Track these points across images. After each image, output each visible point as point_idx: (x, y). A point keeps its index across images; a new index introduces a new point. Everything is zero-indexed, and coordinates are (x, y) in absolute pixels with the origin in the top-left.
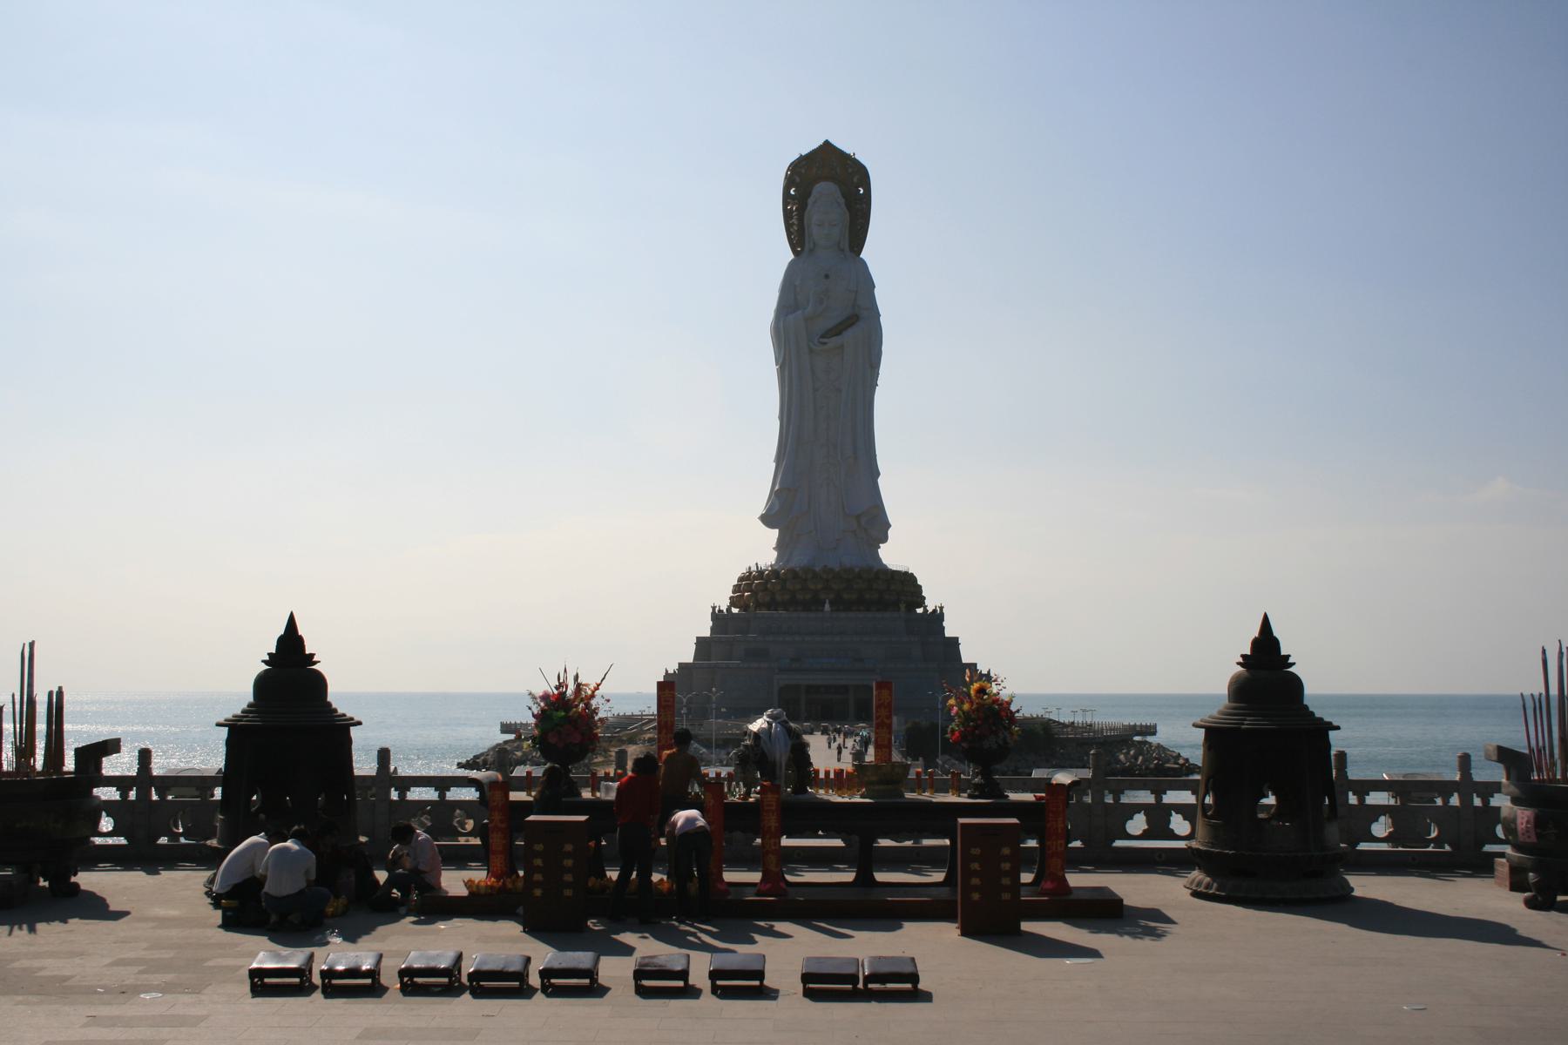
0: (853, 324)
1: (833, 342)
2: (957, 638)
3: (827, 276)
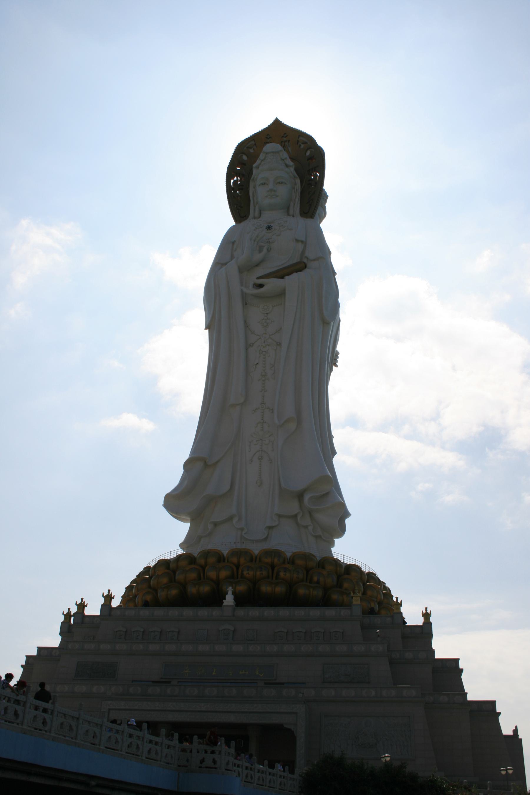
0: (301, 270)
1: (272, 284)
2: (457, 661)
3: (269, 228)
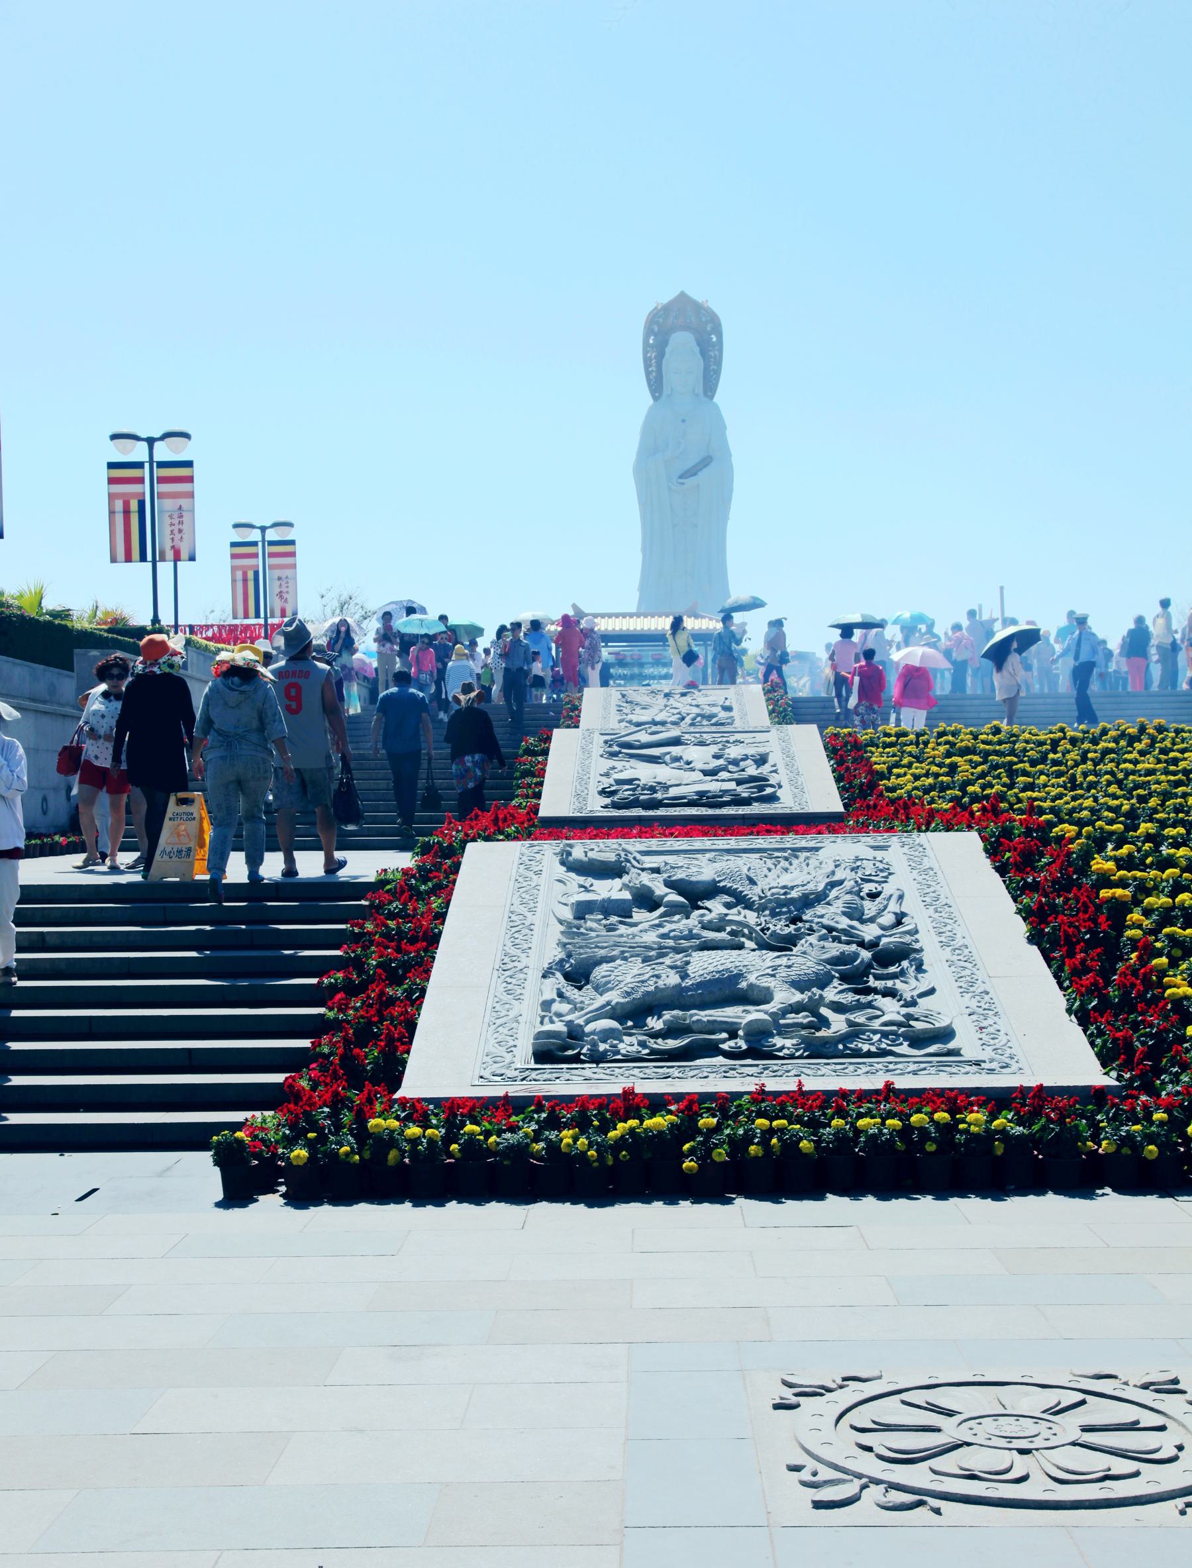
0: (708, 465)
